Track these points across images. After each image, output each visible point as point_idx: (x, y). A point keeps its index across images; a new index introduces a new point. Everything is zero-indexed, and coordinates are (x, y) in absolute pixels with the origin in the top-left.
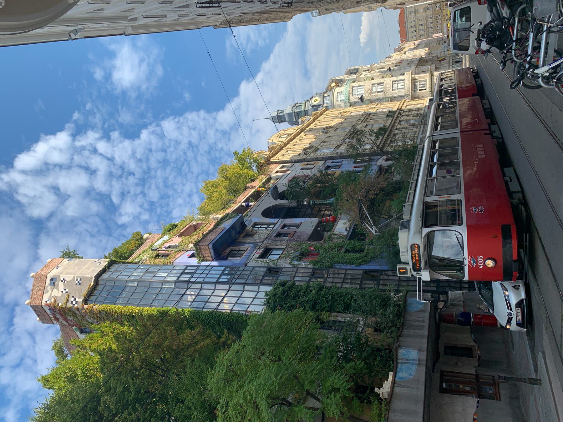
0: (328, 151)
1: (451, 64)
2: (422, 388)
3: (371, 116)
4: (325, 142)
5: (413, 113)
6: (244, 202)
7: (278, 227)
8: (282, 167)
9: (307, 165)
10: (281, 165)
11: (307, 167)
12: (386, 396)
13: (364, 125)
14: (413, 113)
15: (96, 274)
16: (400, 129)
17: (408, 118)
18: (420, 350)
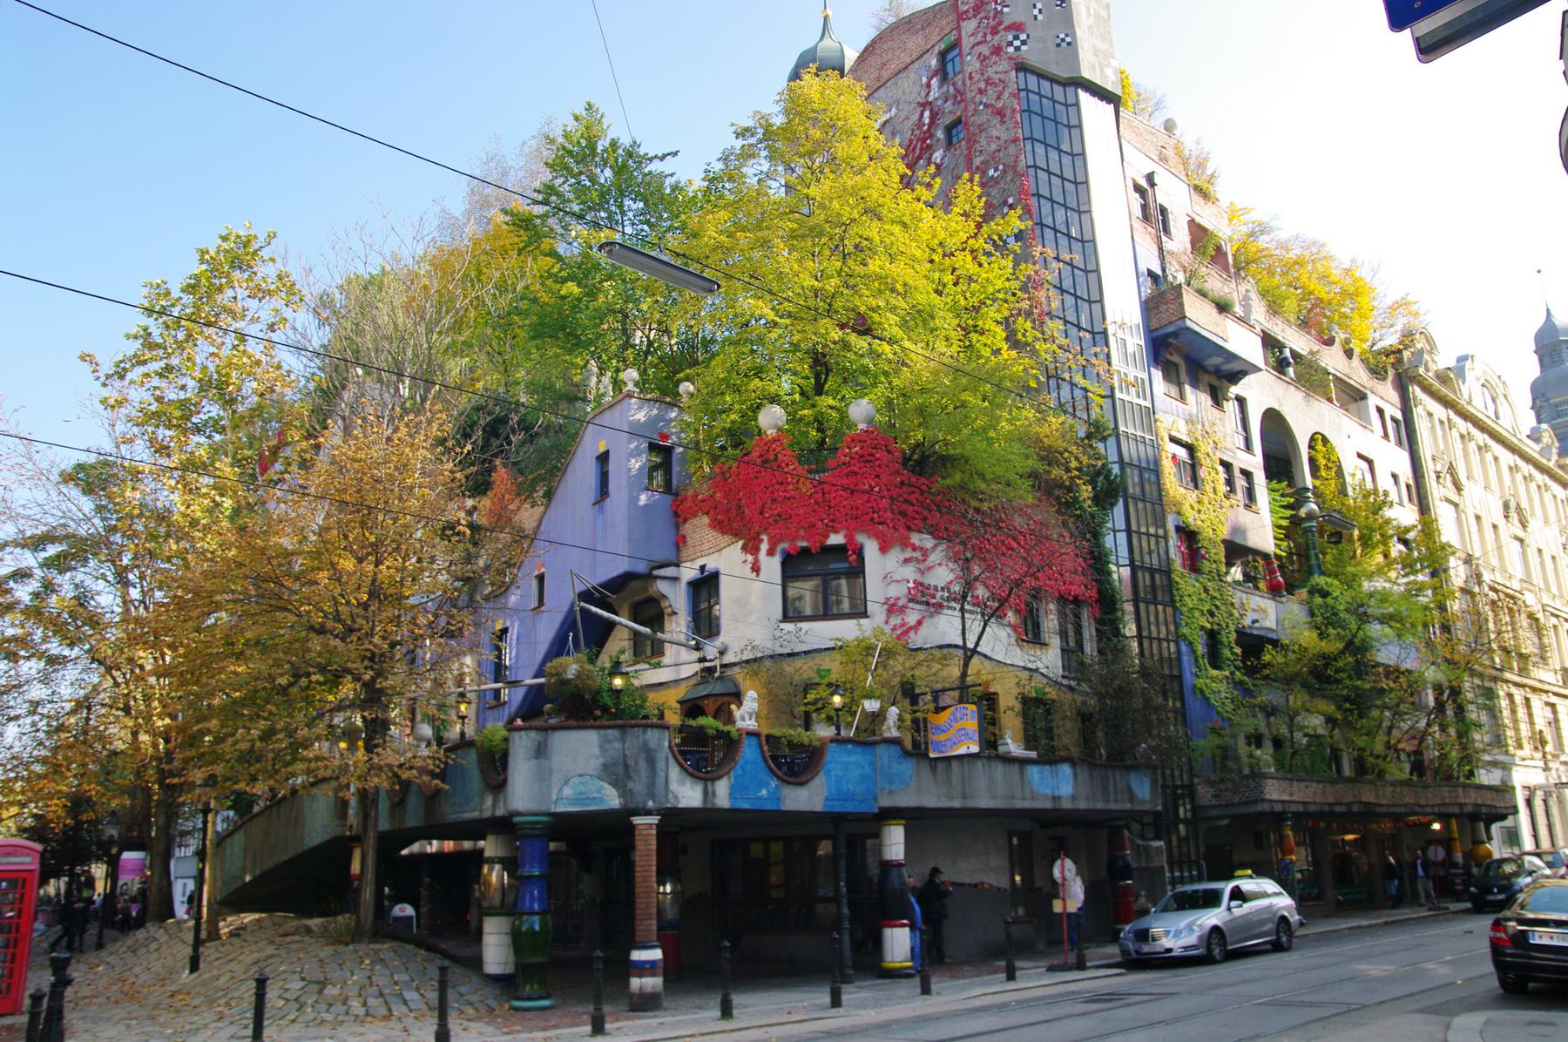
0: (1448, 532)
2: (1027, 804)
4: (1478, 518)
6: (1292, 350)
7: (1242, 460)
8: (1394, 419)
9: (1408, 486)
10: (1399, 416)
12: (1001, 749)
15: (1086, 74)
18: (1073, 798)
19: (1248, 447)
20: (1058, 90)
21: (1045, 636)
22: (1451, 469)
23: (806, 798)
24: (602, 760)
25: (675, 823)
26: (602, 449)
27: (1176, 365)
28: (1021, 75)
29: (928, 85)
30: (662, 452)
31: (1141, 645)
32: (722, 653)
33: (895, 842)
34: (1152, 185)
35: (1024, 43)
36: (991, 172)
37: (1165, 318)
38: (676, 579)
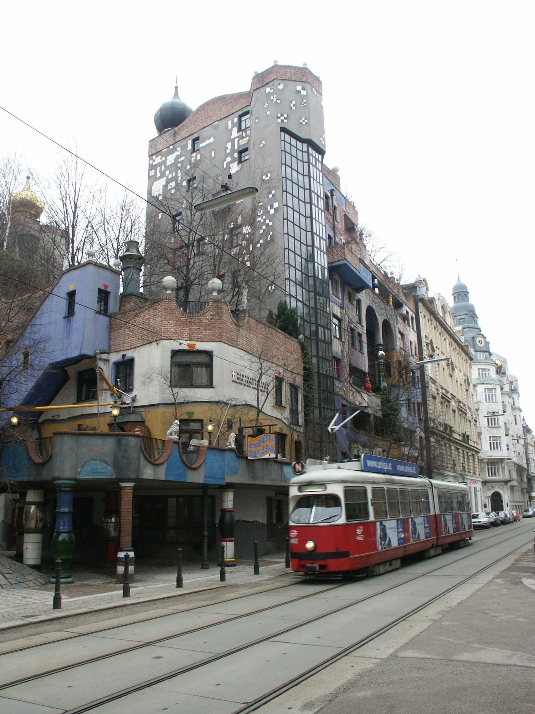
1: (516, 504)
3: (464, 415)
5: (466, 463)
9: (415, 348)
10: (414, 316)
11: (413, 348)
13: (455, 409)
14: (466, 463)
16: (451, 449)
17: (462, 458)
19: (360, 323)
20: (299, 144)
21: (284, 404)
22: (431, 341)
23: (197, 478)
25: (141, 485)
26: (71, 289)
27: (336, 281)
28: (283, 133)
29: (231, 130)
30: (104, 295)
31: (320, 412)
32: (134, 400)
33: (229, 501)
34: (332, 195)
35: (285, 118)
36: (264, 177)
37: (336, 258)
38: (107, 361)
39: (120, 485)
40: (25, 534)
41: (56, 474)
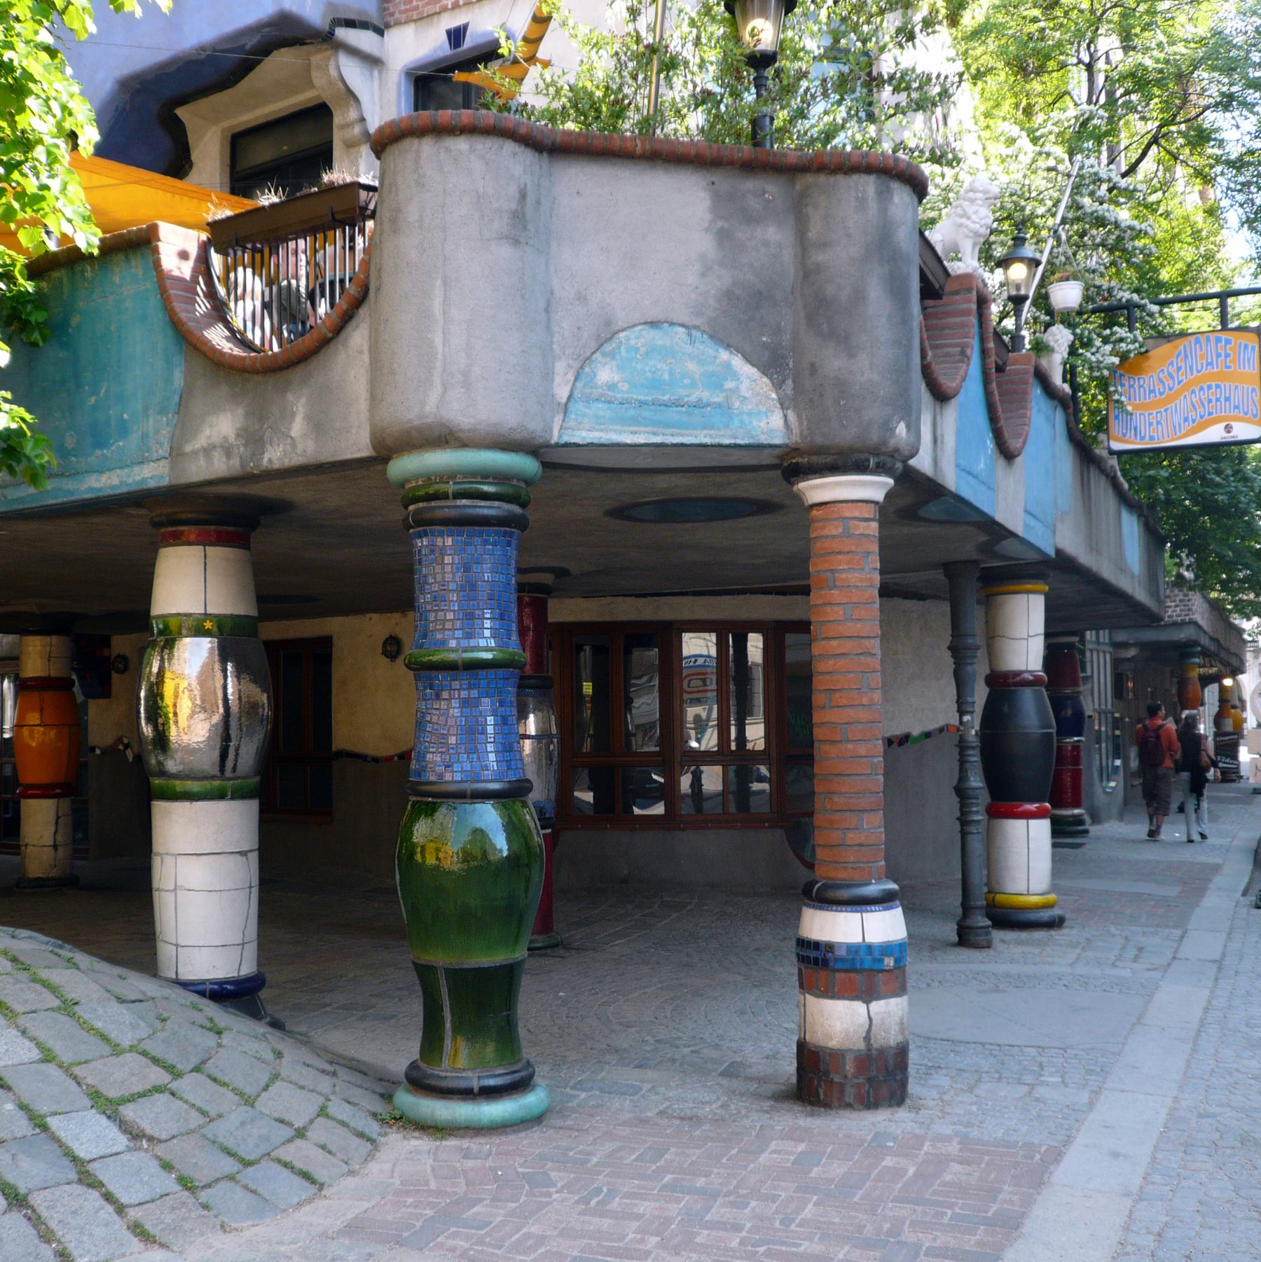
24: (723, 279)
39: (798, 498)
40: (159, 807)
41: (434, 398)
